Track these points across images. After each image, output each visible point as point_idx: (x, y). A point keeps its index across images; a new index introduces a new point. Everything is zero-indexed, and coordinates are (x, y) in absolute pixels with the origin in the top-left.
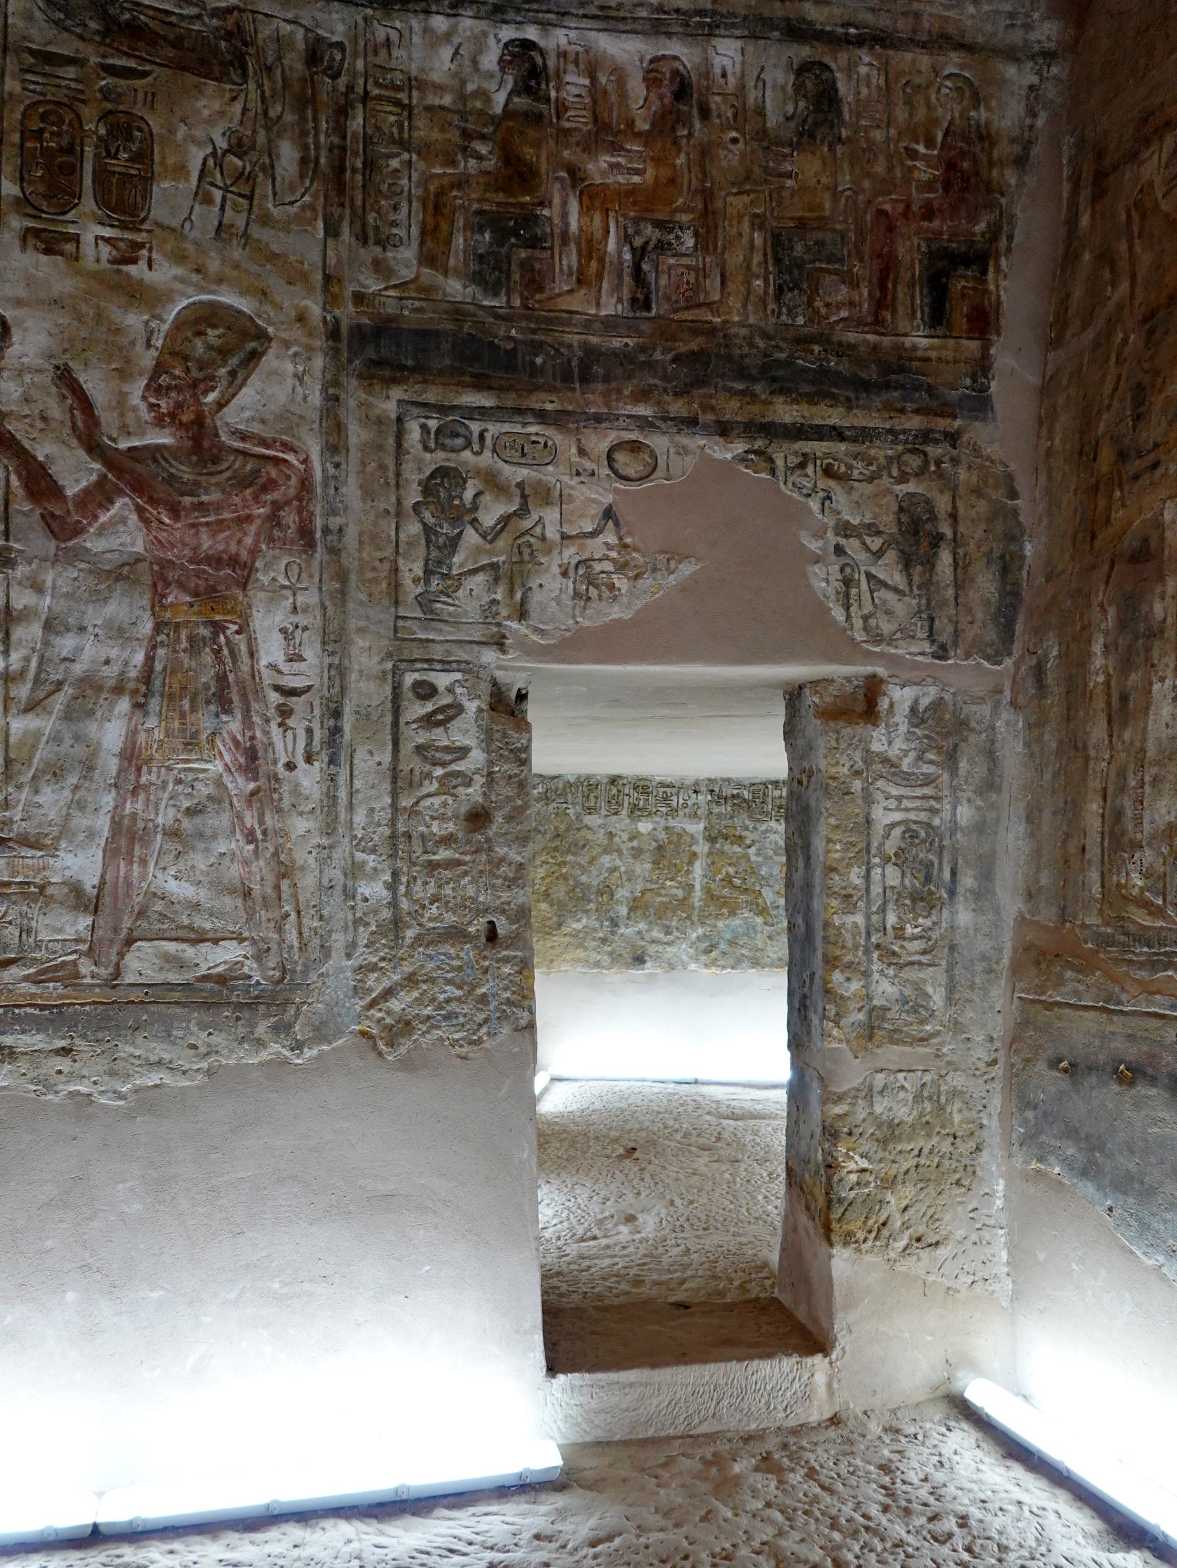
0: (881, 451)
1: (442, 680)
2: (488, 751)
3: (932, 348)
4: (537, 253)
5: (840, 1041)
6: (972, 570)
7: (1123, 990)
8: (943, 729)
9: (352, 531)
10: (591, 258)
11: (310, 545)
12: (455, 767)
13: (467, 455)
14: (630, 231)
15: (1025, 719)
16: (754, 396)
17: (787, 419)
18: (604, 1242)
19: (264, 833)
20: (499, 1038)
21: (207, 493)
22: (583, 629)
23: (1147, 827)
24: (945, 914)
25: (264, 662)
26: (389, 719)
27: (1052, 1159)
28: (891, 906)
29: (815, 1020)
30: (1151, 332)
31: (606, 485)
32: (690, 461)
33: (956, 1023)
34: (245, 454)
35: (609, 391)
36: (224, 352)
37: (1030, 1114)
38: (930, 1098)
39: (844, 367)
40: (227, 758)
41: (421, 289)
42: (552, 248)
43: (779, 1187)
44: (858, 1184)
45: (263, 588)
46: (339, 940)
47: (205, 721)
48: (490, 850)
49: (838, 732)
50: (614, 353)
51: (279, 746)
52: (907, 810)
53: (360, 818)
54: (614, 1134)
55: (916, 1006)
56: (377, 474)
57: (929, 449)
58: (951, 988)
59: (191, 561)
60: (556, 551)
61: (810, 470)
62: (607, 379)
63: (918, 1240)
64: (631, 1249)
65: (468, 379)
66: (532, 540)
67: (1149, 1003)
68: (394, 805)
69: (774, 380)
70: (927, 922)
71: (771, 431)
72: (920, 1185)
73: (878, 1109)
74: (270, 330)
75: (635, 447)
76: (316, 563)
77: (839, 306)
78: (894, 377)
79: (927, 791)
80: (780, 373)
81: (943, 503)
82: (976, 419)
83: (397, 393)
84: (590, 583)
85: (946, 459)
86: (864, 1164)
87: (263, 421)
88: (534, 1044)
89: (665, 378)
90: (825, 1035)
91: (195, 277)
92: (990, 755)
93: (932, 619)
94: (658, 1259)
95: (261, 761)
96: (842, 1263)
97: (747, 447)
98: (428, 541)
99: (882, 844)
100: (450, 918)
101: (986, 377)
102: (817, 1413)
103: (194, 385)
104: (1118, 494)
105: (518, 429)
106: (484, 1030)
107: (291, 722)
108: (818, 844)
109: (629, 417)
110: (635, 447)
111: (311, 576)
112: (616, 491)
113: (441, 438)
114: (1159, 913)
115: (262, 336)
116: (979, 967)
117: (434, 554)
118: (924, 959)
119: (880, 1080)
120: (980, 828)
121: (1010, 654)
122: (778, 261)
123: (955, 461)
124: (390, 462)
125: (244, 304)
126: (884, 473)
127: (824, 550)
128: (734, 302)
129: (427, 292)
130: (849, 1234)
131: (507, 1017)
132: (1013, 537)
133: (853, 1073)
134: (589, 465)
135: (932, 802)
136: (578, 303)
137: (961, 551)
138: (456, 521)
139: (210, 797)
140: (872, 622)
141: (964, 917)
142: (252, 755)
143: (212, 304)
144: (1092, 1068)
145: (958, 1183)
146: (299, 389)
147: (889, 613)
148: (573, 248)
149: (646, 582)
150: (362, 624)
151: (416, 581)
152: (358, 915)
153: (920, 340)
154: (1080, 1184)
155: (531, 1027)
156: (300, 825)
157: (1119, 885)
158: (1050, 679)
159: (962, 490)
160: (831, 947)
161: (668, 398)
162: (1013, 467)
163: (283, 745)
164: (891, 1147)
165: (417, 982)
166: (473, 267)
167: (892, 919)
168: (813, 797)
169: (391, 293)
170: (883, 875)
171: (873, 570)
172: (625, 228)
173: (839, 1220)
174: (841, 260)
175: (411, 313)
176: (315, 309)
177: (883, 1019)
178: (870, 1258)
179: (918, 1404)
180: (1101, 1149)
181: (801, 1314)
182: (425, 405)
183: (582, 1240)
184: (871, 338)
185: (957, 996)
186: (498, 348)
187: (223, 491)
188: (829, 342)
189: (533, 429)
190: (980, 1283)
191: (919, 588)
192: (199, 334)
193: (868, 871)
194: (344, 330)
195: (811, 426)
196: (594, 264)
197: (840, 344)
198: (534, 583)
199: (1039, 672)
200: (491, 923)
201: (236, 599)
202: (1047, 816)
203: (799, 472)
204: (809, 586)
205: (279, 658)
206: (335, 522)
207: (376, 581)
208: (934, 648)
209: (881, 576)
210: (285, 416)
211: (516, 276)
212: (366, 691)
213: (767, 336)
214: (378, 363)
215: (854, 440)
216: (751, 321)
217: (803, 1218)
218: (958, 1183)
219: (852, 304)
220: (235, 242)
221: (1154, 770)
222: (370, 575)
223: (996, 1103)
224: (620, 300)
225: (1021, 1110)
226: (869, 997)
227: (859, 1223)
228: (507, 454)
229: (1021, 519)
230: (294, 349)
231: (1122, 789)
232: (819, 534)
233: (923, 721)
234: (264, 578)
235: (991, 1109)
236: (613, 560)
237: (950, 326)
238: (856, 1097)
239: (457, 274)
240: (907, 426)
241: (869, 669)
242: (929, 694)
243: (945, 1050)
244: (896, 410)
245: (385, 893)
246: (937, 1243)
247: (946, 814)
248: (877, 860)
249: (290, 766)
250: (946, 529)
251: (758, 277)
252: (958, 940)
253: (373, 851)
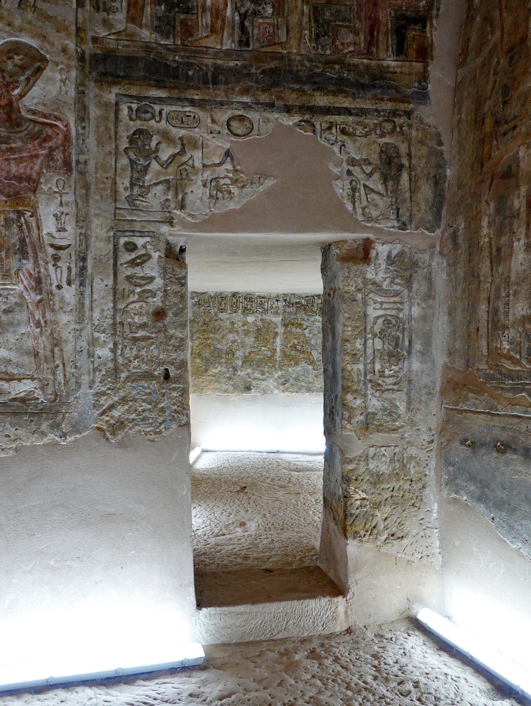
0: (371, 121)
1: (140, 241)
2: (164, 278)
3: (397, 67)
4: (189, 16)
5: (351, 431)
6: (419, 183)
7: (499, 403)
8: (405, 267)
9: (92, 163)
10: (218, 19)
11: (70, 170)
12: (147, 287)
13: (152, 122)
14: (238, 5)
15: (448, 261)
16: (304, 91)
17: (322, 104)
18: (229, 537)
19: (46, 322)
20: (171, 430)
21: (14, 142)
22: (214, 214)
23: (511, 317)
24: (406, 364)
25: (45, 232)
26: (111, 262)
27: (462, 492)
28: (377, 359)
29: (338, 420)
30: (512, 58)
31: (227, 139)
32: (271, 126)
33: (412, 421)
34: (35, 122)
35: (228, 89)
36: (23, 68)
37: (451, 469)
38: (399, 461)
39: (352, 77)
40: (25, 282)
41: (127, 35)
42: (197, 14)
43: (320, 507)
44: (361, 506)
45: (44, 193)
46: (85, 379)
47: (13, 263)
48: (166, 331)
49: (349, 268)
50: (230, 69)
51: (53, 277)
52: (385, 309)
53: (96, 314)
54: (235, 479)
55: (391, 412)
56: (105, 133)
57: (396, 120)
58: (409, 403)
59: (6, 178)
60: (200, 173)
61: (334, 130)
62: (226, 83)
63: (393, 535)
64: (243, 540)
65: (153, 82)
66: (187, 167)
67: (513, 410)
68: (115, 308)
69: (315, 83)
70: (397, 368)
71: (313, 110)
72: (393, 507)
73: (371, 466)
74: (48, 56)
75: (241, 118)
76: (72, 180)
77: (349, 45)
78: (378, 82)
79: (396, 299)
80: (317, 79)
81: (403, 148)
82: (421, 104)
83: (115, 90)
84: (218, 190)
85: (405, 125)
86: (364, 495)
87: (44, 105)
88: (190, 433)
89: (257, 82)
90: (343, 428)
91: (7, 28)
92: (429, 279)
93: (398, 209)
94: (257, 546)
95: (44, 284)
96: (352, 548)
97: (300, 118)
98: (132, 168)
99: (372, 327)
100: (144, 367)
101: (426, 82)
102: (340, 627)
103: (7, 85)
104: (495, 143)
105: (180, 109)
106: (163, 426)
107: (59, 264)
108: (339, 328)
109: (238, 102)
110: (241, 118)
111: (70, 186)
112: (232, 141)
113: (138, 114)
114: (517, 362)
115: (43, 59)
116: (424, 391)
117: (136, 175)
118: (395, 387)
119: (372, 451)
120: (424, 318)
121: (439, 227)
122: (316, 21)
123: (410, 126)
124: (112, 126)
125: (34, 43)
126: (373, 132)
127: (341, 172)
128: (294, 43)
129: (131, 36)
130: (356, 532)
131: (175, 420)
132: (441, 166)
133: (357, 448)
134: (217, 128)
135: (399, 305)
136: (211, 42)
137: (413, 173)
138: (147, 157)
139: (16, 304)
140: (367, 210)
141: (416, 365)
142: (39, 281)
143: (17, 42)
144: (483, 444)
145: (413, 505)
146: (63, 88)
147: (376, 206)
148: (208, 14)
149: (248, 190)
150: (97, 212)
151: (126, 189)
152: (96, 365)
153: (391, 63)
154: (477, 505)
155: (188, 424)
156: (64, 318)
157: (496, 348)
158: (460, 240)
159: (414, 141)
160: (346, 381)
161: (259, 93)
162: (440, 129)
163: (55, 276)
164: (378, 486)
165: (127, 401)
166: (156, 23)
167: (378, 367)
168: (336, 303)
169: (112, 37)
170: (373, 344)
171: (367, 183)
172: (236, 3)
173: (351, 525)
174: (350, 21)
175: (123, 48)
176: (72, 46)
177: (374, 419)
178: (367, 545)
179: (392, 622)
180: (488, 487)
181: (331, 575)
182: (130, 96)
183: (217, 536)
184: (365, 61)
185: (412, 407)
186: (169, 66)
187: (23, 142)
188: (343, 63)
189: (187, 109)
190: (425, 558)
191: (391, 192)
192: (10, 58)
193: (365, 342)
194: (87, 56)
195: (334, 108)
196: (219, 22)
197: (349, 64)
198: (188, 190)
199: (454, 236)
200: (167, 370)
201: (30, 198)
202: (459, 312)
203: (327, 132)
204: (334, 192)
205: (53, 229)
206: (82, 158)
207: (104, 189)
208: (400, 224)
209: (372, 186)
210: (56, 101)
211: (178, 29)
212: (100, 247)
213: (310, 60)
214: (105, 74)
215: (357, 115)
216: (303, 52)
217: (332, 524)
218: (413, 505)
219: (355, 44)
220: (29, 9)
221: (515, 287)
222: (101, 186)
223: (433, 463)
224: (233, 41)
225: (447, 466)
226: (366, 407)
227: (361, 527)
228: (174, 122)
229: (445, 156)
230: (60, 67)
231: (498, 298)
232: (339, 164)
233: (394, 262)
234: (45, 188)
235: (430, 466)
236: (230, 178)
237: (406, 56)
238: (359, 460)
239: (147, 26)
240: (385, 107)
241: (365, 235)
242: (397, 249)
243: (406, 435)
244: (379, 99)
245: (110, 354)
246: (402, 537)
247: (406, 312)
248: (370, 336)
249: (59, 287)
250: (405, 162)
251: (305, 29)
252: (413, 377)
253: (104, 332)
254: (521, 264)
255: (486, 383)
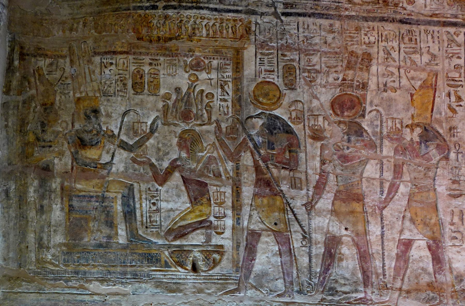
7: (45, 287)
23: (52, 243)
67: (54, 290)
157: (42, 258)
158: (11, 195)
202: (11, 236)
231: (43, 232)
254: (58, 217)
255: (34, 277)
